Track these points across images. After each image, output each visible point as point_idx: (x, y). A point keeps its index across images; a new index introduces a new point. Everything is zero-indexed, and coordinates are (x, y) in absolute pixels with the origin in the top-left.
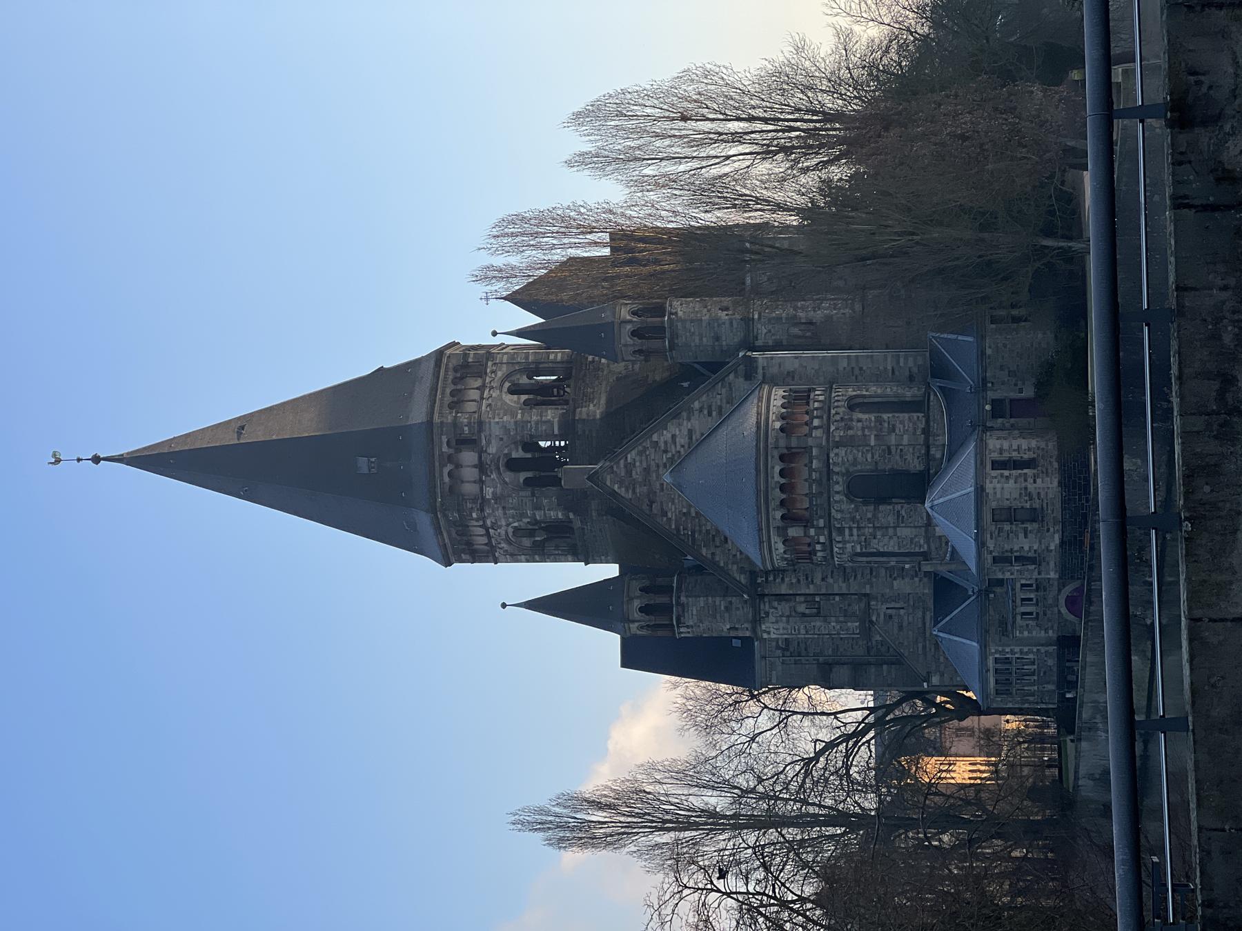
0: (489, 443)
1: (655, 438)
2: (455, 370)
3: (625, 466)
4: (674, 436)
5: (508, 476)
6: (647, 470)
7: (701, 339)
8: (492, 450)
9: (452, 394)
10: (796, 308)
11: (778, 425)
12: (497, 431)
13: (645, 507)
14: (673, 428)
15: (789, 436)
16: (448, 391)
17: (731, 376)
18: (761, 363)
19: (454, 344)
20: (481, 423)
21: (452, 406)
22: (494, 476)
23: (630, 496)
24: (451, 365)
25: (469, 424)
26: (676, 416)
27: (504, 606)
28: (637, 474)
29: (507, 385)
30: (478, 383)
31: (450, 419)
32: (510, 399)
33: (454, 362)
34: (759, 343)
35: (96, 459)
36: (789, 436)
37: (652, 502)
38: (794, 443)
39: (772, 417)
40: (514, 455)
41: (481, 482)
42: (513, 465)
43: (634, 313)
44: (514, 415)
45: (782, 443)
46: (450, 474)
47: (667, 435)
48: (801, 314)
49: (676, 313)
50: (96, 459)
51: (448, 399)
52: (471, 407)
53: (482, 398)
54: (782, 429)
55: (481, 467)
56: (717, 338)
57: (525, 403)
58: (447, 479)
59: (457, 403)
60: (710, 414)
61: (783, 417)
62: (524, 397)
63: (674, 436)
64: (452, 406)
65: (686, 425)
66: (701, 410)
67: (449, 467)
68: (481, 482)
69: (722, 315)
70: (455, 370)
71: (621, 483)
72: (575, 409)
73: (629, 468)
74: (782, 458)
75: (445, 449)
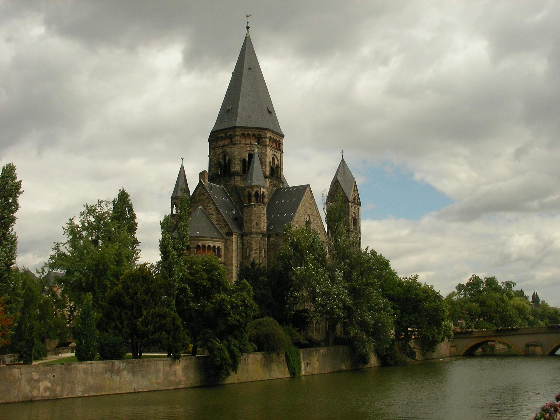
0: (230, 148)
1: (211, 202)
2: (259, 135)
3: (204, 193)
4: (211, 209)
5: (221, 156)
6: (203, 200)
7: (247, 217)
8: (228, 150)
9: (249, 135)
10: (256, 250)
11: (200, 244)
12: (233, 150)
15: (195, 248)
16: (250, 133)
17: (227, 228)
18: (231, 238)
19: (283, 137)
20: (235, 144)
21: (243, 134)
22: (221, 151)
23: (196, 195)
24: (261, 133)
25: (235, 140)
27: (182, 159)
29: (253, 153)
31: (237, 134)
32: (247, 155)
33: (262, 134)
34: (244, 237)
35: (248, 28)
36: (195, 248)
37: (194, 203)
39: (204, 242)
41: (219, 147)
42: (225, 157)
43: (257, 192)
45: (192, 246)
46: (222, 136)
48: (253, 252)
49: (255, 207)
50: (248, 28)
51: (246, 133)
52: (243, 142)
53: (246, 144)
54: (198, 246)
56: (246, 222)
57: (244, 160)
58: (220, 135)
60: (217, 221)
62: (247, 159)
63: (211, 209)
64: (243, 134)
65: (214, 213)
67: (223, 135)
68: (219, 147)
71: (200, 192)
72: (240, 176)
73: (203, 194)
75: (229, 133)
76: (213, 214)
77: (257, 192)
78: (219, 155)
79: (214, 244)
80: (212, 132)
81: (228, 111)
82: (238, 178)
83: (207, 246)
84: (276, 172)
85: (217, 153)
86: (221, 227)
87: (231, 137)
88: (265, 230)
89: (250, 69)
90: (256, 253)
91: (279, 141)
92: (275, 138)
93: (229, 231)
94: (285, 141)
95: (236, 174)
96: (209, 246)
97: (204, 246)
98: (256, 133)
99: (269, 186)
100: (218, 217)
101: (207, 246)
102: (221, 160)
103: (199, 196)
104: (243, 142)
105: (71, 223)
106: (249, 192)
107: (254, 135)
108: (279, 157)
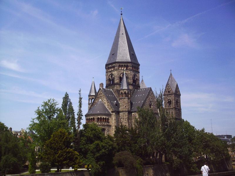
2: (127, 65)
3: (102, 93)
5: (110, 76)
6: (101, 97)
8: (113, 73)
9: (122, 65)
10: (125, 119)
11: (99, 117)
13: (97, 97)
14: (106, 100)
16: (123, 64)
19: (139, 65)
21: (120, 65)
22: (110, 73)
26: (107, 101)
28: (101, 95)
30: (125, 69)
37: (97, 98)
38: (96, 120)
39: (101, 116)
40: (113, 76)
42: (112, 77)
44: (117, 75)
45: (95, 118)
46: (110, 67)
47: (105, 99)
49: (124, 99)
50: (122, 14)
51: (121, 64)
55: (112, 71)
59: (119, 66)
60: (108, 106)
61: (101, 118)
64: (120, 65)
65: (106, 102)
66: (108, 104)
67: (111, 66)
69: (124, 107)
70: (127, 65)
71: (100, 93)
73: (101, 94)
74: (94, 118)
75: (113, 65)
76: (105, 103)
77: (125, 92)
78: (109, 75)
79: (106, 117)
80: (106, 65)
81: (113, 54)
82: (118, 86)
83: (102, 118)
84: (135, 83)
85: (109, 74)
86: (109, 109)
87: (114, 67)
88: (130, 110)
89: (123, 34)
90: (125, 120)
91: (137, 67)
92: (135, 66)
93: (113, 110)
94: (140, 67)
95: (117, 84)
96: (103, 118)
97: (101, 118)
98: (126, 64)
99: (133, 89)
100: (108, 104)
101: (102, 118)
102: (110, 78)
103: (100, 95)
104: (120, 68)
105: (38, 110)
106: (122, 92)
107: (125, 65)
108: (137, 75)
